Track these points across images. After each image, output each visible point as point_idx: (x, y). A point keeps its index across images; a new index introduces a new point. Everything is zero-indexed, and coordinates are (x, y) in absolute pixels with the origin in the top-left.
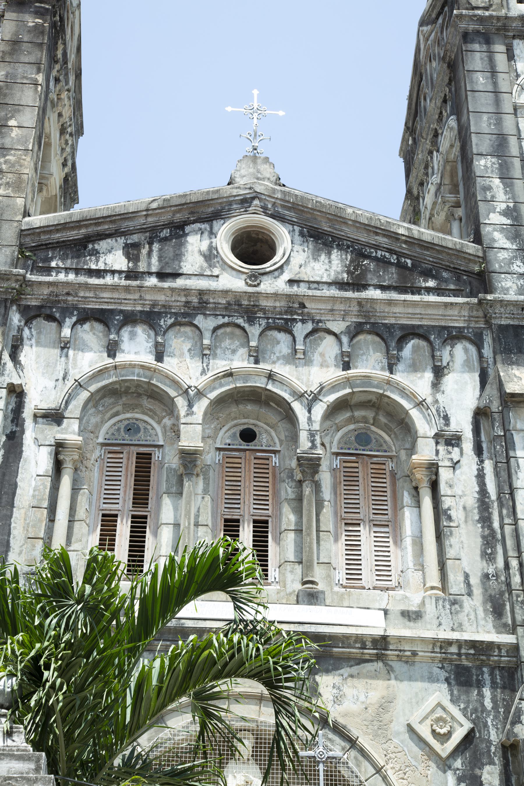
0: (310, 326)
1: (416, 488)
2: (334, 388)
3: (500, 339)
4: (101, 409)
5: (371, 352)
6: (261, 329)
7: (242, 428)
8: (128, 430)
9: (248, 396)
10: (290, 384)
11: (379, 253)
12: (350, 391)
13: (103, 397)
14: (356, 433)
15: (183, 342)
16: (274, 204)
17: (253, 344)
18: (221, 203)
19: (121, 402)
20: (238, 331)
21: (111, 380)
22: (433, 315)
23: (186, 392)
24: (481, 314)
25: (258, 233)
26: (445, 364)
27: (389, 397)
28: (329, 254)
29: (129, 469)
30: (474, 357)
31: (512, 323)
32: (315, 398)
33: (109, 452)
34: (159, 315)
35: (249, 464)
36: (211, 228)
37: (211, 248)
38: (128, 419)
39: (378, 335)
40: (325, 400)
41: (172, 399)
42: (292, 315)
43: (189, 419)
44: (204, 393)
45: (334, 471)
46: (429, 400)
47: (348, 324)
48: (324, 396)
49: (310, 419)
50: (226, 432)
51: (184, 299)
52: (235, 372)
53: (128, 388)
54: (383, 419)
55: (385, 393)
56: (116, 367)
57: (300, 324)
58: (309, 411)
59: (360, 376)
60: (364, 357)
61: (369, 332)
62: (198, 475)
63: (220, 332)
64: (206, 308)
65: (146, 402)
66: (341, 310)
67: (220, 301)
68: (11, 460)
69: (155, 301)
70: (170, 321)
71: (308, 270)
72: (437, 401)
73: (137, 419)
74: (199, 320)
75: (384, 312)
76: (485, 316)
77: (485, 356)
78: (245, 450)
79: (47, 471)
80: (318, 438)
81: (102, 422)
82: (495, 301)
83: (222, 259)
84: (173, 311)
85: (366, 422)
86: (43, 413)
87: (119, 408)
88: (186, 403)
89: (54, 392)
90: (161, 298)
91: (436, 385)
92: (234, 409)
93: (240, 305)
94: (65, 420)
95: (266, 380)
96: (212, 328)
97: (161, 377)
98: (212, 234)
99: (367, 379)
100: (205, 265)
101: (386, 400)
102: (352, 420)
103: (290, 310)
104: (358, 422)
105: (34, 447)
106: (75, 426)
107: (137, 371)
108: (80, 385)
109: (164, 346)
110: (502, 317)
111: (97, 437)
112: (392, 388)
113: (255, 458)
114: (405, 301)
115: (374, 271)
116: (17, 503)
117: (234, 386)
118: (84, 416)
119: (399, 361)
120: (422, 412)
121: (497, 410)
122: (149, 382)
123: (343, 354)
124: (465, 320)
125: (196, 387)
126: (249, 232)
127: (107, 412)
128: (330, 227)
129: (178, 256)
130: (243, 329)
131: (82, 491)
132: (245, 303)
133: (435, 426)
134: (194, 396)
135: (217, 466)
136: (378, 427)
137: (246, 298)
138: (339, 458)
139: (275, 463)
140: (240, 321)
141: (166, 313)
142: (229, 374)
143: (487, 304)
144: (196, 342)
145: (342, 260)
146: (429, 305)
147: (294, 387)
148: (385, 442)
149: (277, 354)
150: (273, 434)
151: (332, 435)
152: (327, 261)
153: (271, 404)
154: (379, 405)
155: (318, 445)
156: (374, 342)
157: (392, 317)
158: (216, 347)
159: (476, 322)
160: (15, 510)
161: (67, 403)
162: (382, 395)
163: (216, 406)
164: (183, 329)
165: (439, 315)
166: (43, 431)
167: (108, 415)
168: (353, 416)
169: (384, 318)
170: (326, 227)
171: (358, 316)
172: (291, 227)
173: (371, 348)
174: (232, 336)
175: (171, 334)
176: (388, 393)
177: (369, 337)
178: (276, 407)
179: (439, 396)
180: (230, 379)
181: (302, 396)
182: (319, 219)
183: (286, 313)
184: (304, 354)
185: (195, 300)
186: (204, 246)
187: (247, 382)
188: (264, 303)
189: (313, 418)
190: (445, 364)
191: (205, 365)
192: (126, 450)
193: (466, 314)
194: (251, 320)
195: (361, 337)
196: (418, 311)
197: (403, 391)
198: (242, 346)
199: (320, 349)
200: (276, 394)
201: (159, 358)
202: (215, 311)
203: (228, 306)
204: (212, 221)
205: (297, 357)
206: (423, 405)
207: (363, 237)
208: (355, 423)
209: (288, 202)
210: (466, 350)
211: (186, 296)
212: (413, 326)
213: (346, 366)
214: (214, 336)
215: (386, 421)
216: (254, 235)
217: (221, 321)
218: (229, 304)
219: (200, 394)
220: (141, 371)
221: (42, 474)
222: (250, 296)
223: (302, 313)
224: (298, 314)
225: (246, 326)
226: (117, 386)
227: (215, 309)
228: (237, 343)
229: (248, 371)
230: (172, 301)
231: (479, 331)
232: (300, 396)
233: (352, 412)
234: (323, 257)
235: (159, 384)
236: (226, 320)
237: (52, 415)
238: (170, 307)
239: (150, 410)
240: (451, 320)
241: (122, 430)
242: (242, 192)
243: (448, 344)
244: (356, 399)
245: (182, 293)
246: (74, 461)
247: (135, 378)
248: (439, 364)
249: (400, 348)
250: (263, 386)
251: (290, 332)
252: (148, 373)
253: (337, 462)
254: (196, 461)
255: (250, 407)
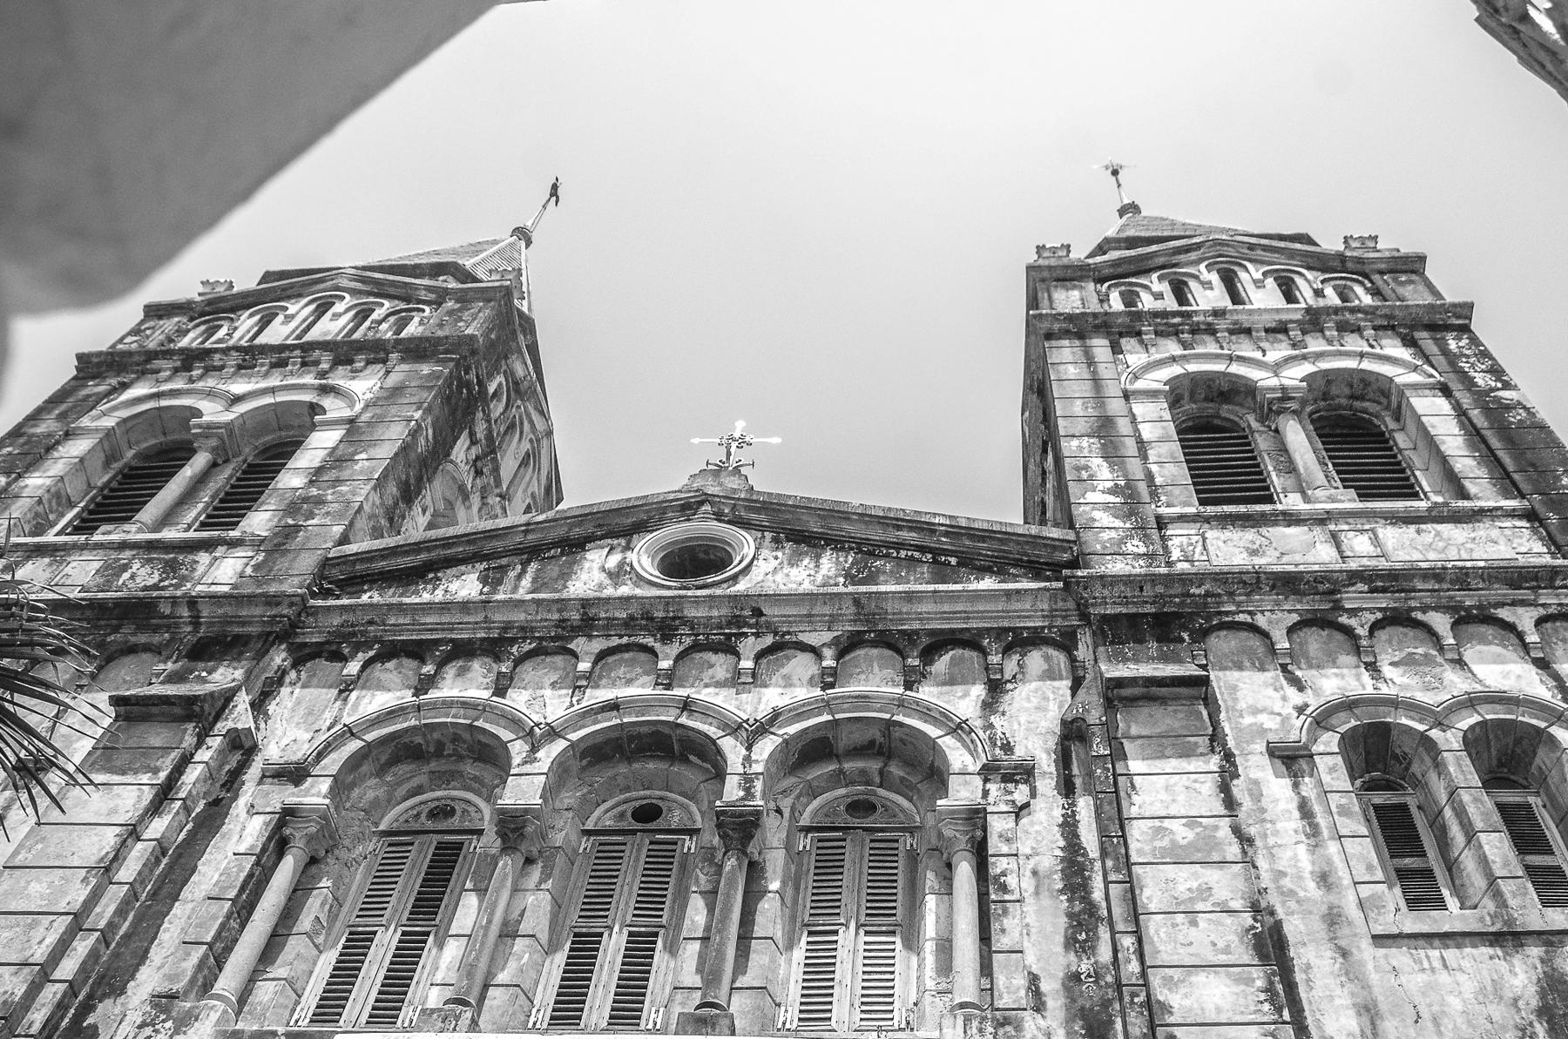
0: (769, 640)
1: (949, 866)
2: (798, 712)
3: (1102, 630)
4: (388, 779)
5: (876, 669)
6: (682, 648)
7: (637, 804)
8: (433, 815)
9: (650, 750)
10: (719, 713)
11: (903, 554)
12: (830, 718)
13: (395, 760)
14: (849, 800)
15: (546, 674)
16: (734, 506)
17: (665, 664)
18: (647, 512)
19: (425, 769)
20: (643, 656)
21: (405, 725)
22: (988, 612)
23: (531, 732)
24: (1071, 605)
25: (707, 549)
26: (1007, 676)
27: (901, 725)
28: (818, 557)
29: (418, 865)
30: (1062, 666)
31: (1125, 611)
32: (762, 729)
33: (390, 845)
34: (513, 641)
35: (639, 850)
36: (629, 543)
37: (622, 564)
38: (438, 799)
39: (890, 646)
40: (781, 732)
41: (504, 745)
42: (740, 628)
43: (528, 768)
44: (563, 733)
45: (793, 855)
46: (977, 723)
47: (836, 634)
48: (780, 727)
49: (747, 760)
50: (607, 811)
51: (556, 616)
52: (624, 703)
53: (440, 746)
54: (896, 770)
55: (895, 718)
56: (419, 708)
57: (751, 639)
58: (749, 748)
59: (849, 697)
60: (863, 677)
61: (874, 644)
62: (529, 861)
63: (611, 659)
64: (592, 628)
65: (470, 768)
66: (825, 615)
67: (617, 615)
68: (199, 837)
69: (509, 622)
70: (527, 647)
71: (779, 577)
72: (991, 726)
73: (453, 799)
74: (578, 644)
75: (900, 613)
76: (1078, 605)
77: (1080, 658)
78: (634, 832)
79: (252, 847)
80: (759, 785)
81: (389, 801)
82: (1091, 577)
83: (638, 575)
84: (537, 635)
85: (868, 783)
86: (276, 770)
87: (421, 779)
88: (527, 748)
89: (306, 746)
90: (519, 617)
91: (989, 707)
92: (623, 769)
93: (652, 619)
94: (310, 779)
95: (678, 711)
96: (597, 651)
97: (493, 716)
98: (628, 548)
99: (863, 699)
100: (608, 581)
101: (897, 733)
102: (839, 778)
103: (737, 621)
104: (852, 783)
105: (243, 815)
106: (325, 786)
107: (453, 711)
108: (350, 732)
109: (512, 679)
110: (1106, 603)
111: (376, 824)
112: (908, 711)
113: (651, 843)
114: (935, 592)
115: (891, 572)
116: (185, 893)
117: (619, 721)
118: (352, 786)
119: (925, 677)
120: (961, 740)
121: (1098, 721)
122: (470, 725)
123: (825, 672)
124: (1043, 616)
125: (547, 724)
126: (692, 548)
127: (399, 784)
128: (822, 527)
129: (566, 576)
130: (651, 651)
131: (315, 892)
132: (661, 614)
133: (983, 755)
134: (542, 736)
135: (580, 857)
136: (889, 789)
137: (661, 607)
138: (810, 835)
139: (689, 849)
140: (649, 641)
141: (524, 639)
142: (613, 706)
143: (1078, 583)
144: (568, 674)
145: (838, 562)
146: (978, 596)
147: (725, 718)
148: (903, 810)
149: (706, 680)
150: (694, 808)
151: (798, 797)
152: (812, 565)
153: (692, 757)
154: (890, 747)
155: (758, 794)
156: (881, 657)
157: (915, 619)
158: (600, 677)
159: (1064, 618)
160: (177, 904)
161: (320, 755)
162: (890, 724)
163: (590, 764)
164: (548, 659)
165: (998, 611)
166: (268, 794)
167: (401, 791)
168: (841, 771)
169: (902, 621)
170: (815, 526)
171: (855, 621)
172: (759, 534)
173: (875, 664)
174: (632, 663)
175: (527, 666)
176: (899, 718)
177: (875, 652)
178: (699, 762)
179: (995, 720)
180: (615, 713)
181: (740, 726)
182: (804, 517)
183: (729, 624)
184: (754, 675)
185: (575, 616)
186: (613, 561)
187: (643, 715)
188: (691, 612)
189: (754, 757)
190: (1007, 676)
191: (575, 699)
192: (418, 840)
193: (1046, 606)
194: (667, 638)
195: (861, 652)
196: (960, 607)
197: (927, 713)
198: (647, 673)
199: (784, 671)
200: (693, 729)
201: (500, 691)
202: (608, 630)
203: (629, 624)
204: (631, 535)
205: (742, 680)
206: (962, 728)
207: (876, 534)
208: (847, 786)
209: (756, 501)
210: (1047, 658)
211: (560, 611)
212: (952, 631)
213: (826, 686)
214: (600, 664)
215: (902, 774)
216: (702, 556)
217: (615, 641)
218: (632, 618)
219: (553, 733)
220: (462, 711)
221: (242, 851)
222: (668, 603)
223: (757, 623)
224: (750, 626)
225: (657, 646)
226: (419, 740)
227: (606, 627)
228: (639, 670)
229: (647, 700)
230: (537, 621)
231: (1070, 630)
232: (734, 729)
233: (839, 762)
234: (806, 561)
235: (487, 726)
236: (625, 640)
237: (291, 772)
238: (533, 629)
239: (475, 779)
240: (1019, 617)
241: (423, 816)
242: (683, 495)
243: (1016, 653)
244: (845, 740)
245: (554, 608)
246: (310, 839)
247: (449, 720)
248: (998, 677)
249: (931, 663)
250: (671, 719)
251: (730, 649)
252: (471, 713)
253: (804, 842)
254: (523, 827)
255: (651, 766)
